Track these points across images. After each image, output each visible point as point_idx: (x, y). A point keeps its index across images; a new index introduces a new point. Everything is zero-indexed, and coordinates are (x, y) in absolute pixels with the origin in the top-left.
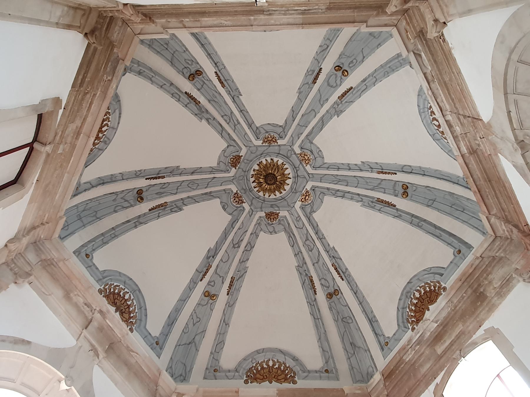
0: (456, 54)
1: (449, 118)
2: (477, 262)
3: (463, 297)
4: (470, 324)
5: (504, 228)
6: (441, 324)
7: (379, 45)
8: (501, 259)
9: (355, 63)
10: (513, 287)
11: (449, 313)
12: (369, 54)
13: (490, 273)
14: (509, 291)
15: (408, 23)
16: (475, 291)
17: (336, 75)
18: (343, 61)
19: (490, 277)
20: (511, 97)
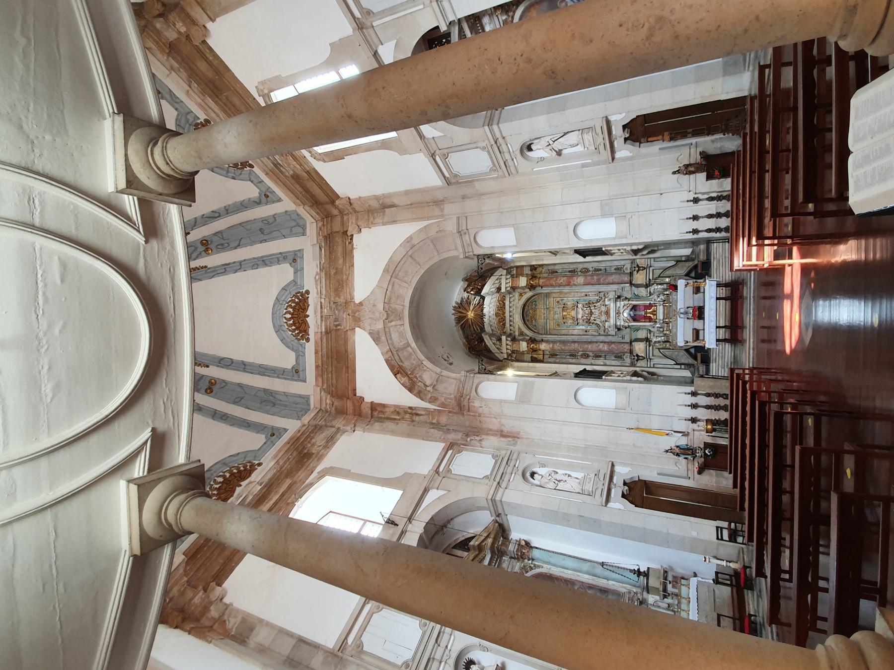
0: (356, 253)
1: (323, 301)
2: (304, 428)
3: (288, 459)
4: (301, 475)
5: (328, 401)
6: (265, 486)
7: (266, 241)
8: (321, 427)
9: (223, 246)
10: (337, 440)
11: (275, 474)
12: (246, 245)
13: (313, 438)
14: (334, 443)
15: (323, 225)
16: (300, 453)
17: (196, 248)
18: (215, 239)
19: (313, 441)
20: (393, 279)
